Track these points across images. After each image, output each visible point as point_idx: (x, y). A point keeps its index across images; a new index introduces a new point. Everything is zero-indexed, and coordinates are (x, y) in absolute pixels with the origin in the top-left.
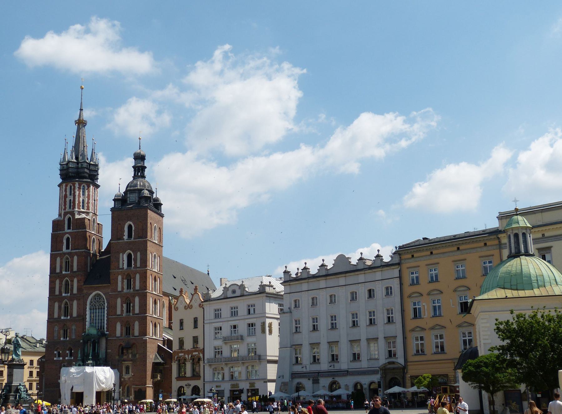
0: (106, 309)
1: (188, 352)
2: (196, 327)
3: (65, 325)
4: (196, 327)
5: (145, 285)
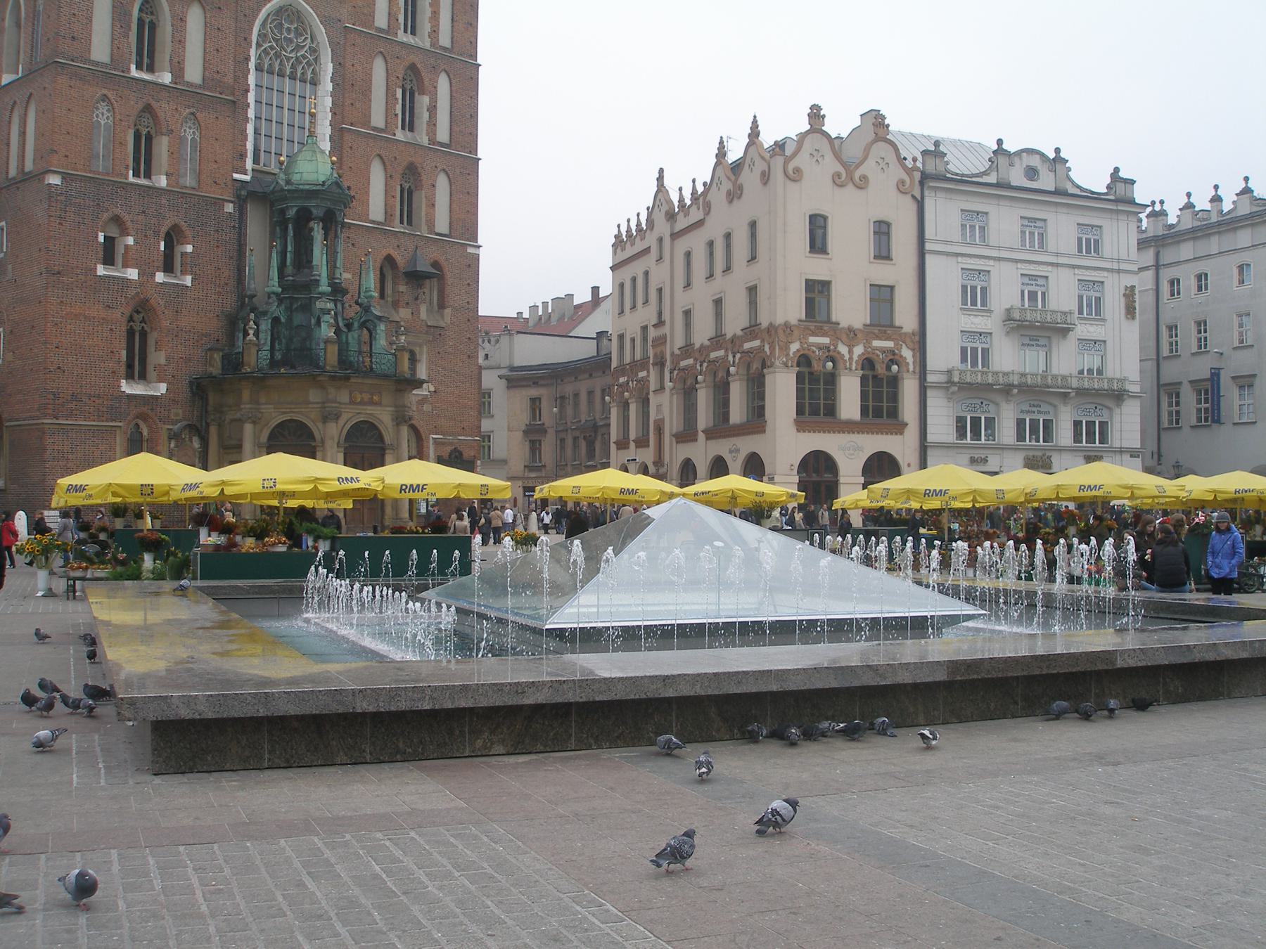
0: (330, 87)
1: (852, 335)
2: (883, 254)
3: (148, 109)
4: (883, 254)
5: (472, 39)
